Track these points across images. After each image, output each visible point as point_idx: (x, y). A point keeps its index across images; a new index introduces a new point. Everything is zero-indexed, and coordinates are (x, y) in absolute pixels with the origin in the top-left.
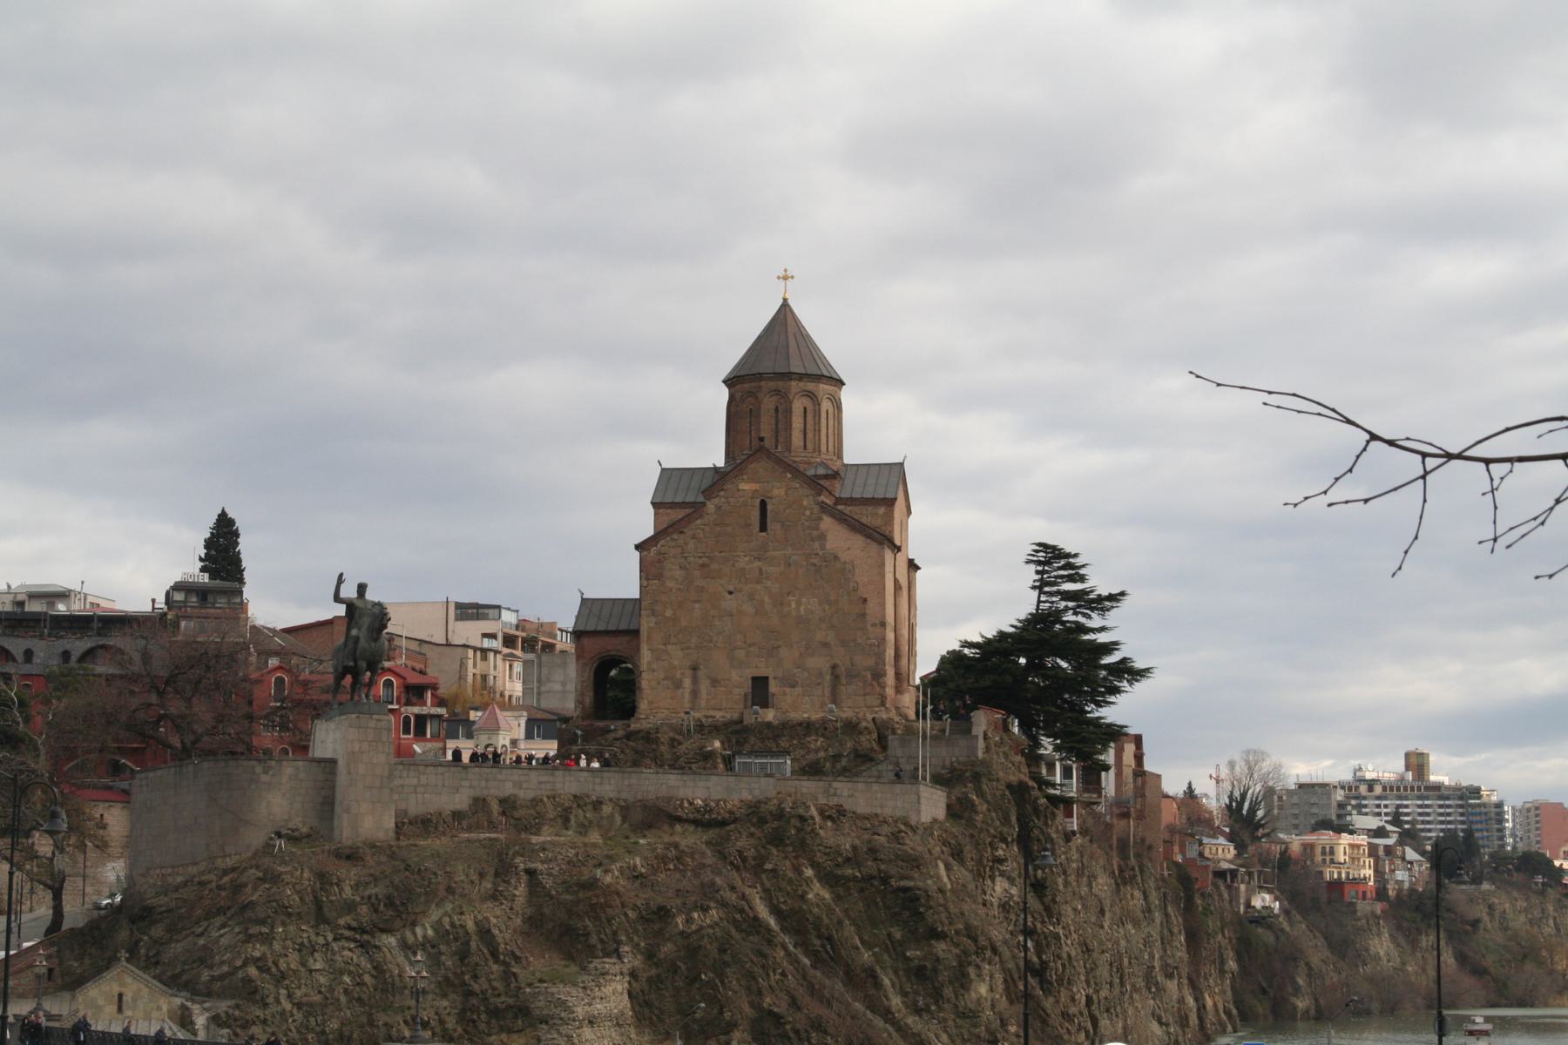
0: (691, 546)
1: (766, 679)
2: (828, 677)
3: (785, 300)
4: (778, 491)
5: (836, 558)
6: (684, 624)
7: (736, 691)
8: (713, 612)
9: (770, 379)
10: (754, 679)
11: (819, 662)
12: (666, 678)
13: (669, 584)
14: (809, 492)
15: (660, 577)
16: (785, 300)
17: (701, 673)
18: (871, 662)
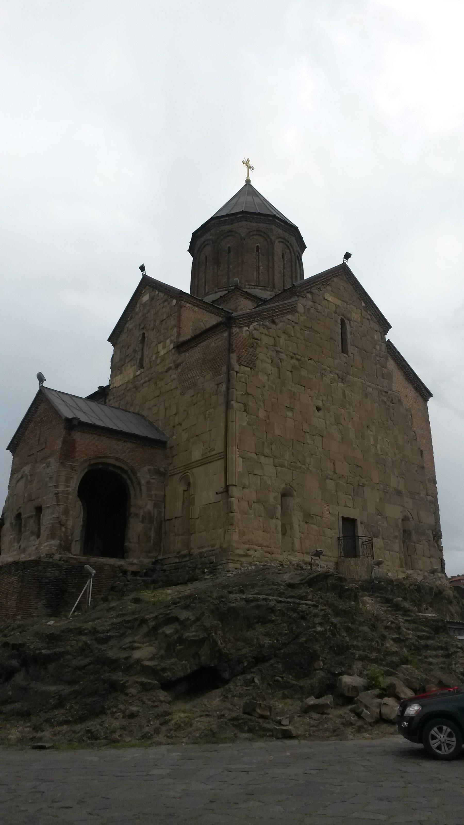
0: (282, 341)
1: (353, 521)
2: (401, 531)
3: (248, 182)
4: (356, 316)
5: (400, 401)
6: (278, 432)
7: (328, 532)
8: (306, 427)
9: (278, 226)
10: (344, 519)
11: (394, 512)
12: (258, 501)
13: (263, 378)
14: (377, 327)
15: (251, 365)
16: (248, 182)
17: (292, 502)
18: (431, 520)
